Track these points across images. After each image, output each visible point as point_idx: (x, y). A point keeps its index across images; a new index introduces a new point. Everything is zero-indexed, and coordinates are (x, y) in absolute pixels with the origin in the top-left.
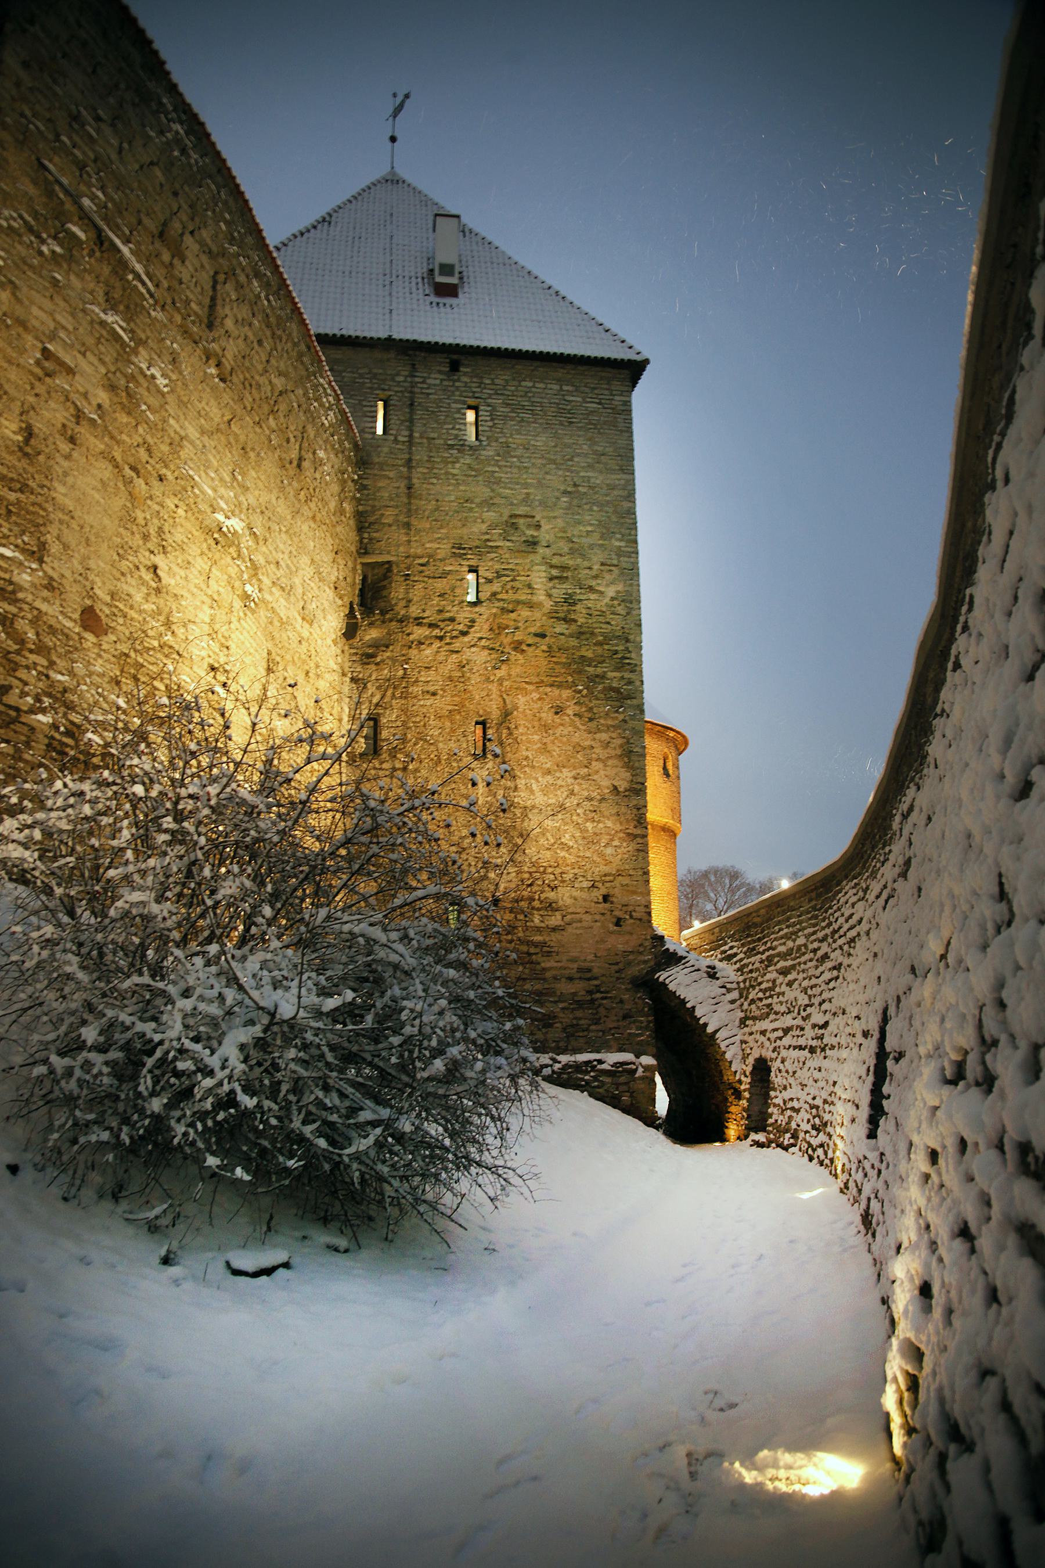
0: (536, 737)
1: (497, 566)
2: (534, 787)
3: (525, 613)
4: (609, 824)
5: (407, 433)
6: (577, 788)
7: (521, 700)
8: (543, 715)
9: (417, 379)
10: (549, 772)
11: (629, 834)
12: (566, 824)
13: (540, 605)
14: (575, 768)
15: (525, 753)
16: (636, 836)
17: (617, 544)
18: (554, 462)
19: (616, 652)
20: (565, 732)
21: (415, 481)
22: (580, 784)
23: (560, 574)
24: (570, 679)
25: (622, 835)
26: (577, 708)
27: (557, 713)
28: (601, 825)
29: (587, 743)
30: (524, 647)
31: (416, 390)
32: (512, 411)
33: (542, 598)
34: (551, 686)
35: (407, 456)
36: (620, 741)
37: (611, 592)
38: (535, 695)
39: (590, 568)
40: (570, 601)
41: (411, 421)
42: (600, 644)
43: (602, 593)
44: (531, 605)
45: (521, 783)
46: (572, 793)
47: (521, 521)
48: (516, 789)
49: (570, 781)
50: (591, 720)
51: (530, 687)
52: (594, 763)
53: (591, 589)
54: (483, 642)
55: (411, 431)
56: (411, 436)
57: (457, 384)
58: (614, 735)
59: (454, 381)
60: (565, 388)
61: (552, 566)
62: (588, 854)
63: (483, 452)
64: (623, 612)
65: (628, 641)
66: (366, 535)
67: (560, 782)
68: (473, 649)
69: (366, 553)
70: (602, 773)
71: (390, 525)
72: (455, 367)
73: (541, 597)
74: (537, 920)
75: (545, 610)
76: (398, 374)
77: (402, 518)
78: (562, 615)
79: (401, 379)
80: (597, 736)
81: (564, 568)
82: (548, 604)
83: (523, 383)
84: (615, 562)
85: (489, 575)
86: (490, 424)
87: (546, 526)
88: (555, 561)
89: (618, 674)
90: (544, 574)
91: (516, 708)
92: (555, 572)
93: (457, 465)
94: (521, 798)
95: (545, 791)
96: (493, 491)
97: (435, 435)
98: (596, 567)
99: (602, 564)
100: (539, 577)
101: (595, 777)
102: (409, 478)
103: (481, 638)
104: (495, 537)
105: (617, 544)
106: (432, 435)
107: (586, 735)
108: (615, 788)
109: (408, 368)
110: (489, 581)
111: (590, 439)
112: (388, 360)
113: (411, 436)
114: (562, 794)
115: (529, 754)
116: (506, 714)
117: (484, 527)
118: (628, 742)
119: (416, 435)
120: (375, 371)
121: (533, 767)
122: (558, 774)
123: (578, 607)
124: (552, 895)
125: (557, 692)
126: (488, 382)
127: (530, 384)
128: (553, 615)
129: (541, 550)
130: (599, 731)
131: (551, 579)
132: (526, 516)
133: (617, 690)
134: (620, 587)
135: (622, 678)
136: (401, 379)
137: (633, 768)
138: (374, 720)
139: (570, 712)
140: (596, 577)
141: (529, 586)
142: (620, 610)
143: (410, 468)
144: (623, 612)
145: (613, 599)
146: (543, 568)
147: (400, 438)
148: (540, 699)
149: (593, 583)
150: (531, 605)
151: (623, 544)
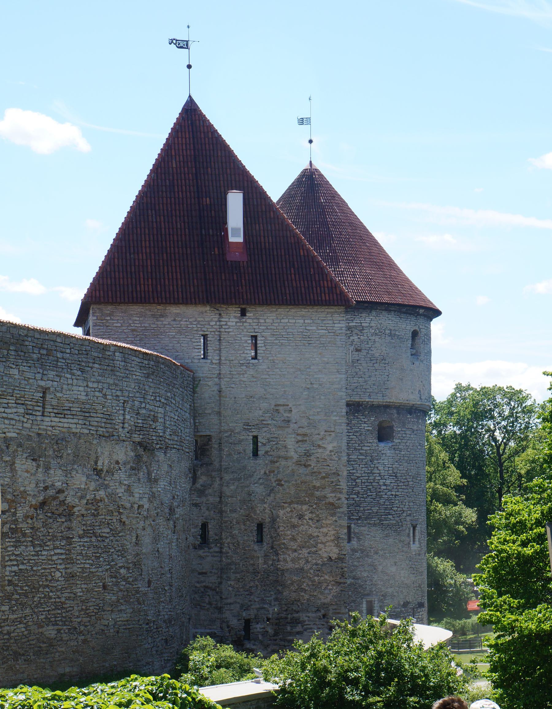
0: (289, 532)
1: (268, 436)
2: (288, 559)
3: (283, 463)
4: (327, 577)
5: (218, 358)
6: (310, 559)
7: (281, 513)
8: (293, 520)
9: (222, 323)
10: (295, 551)
11: (337, 582)
12: (304, 578)
13: (291, 458)
14: (309, 548)
15: (283, 541)
16: (340, 583)
17: (334, 418)
18: (300, 370)
19: (332, 482)
20: (304, 529)
21: (223, 386)
22: (311, 557)
23: (302, 439)
24: (307, 499)
25: (333, 583)
26: (310, 515)
27: (300, 518)
28: (322, 578)
29: (316, 534)
30: (283, 483)
31: (222, 330)
32: (276, 339)
33: (292, 453)
34: (298, 504)
35: (218, 372)
36: (333, 532)
37: (330, 447)
38: (288, 509)
39: (319, 434)
40: (308, 454)
41: (220, 350)
42: (323, 478)
43: (325, 448)
44: (286, 458)
45: (281, 557)
46: (307, 562)
47: (281, 408)
48: (279, 560)
49: (306, 555)
50: (318, 521)
51: (286, 505)
52: (319, 545)
53: (319, 446)
54: (261, 481)
55: (220, 356)
56: (220, 359)
57: (245, 324)
58: (330, 529)
59: (243, 322)
60: (306, 321)
61: (298, 435)
62: (315, 594)
63: (260, 367)
64: (337, 459)
65: (339, 475)
66: (197, 421)
67: (301, 556)
68: (256, 485)
69: (198, 431)
70: (323, 550)
71: (210, 414)
72: (243, 313)
73: (292, 453)
74: (289, 628)
75: (294, 461)
76: (212, 321)
77: (216, 409)
78: (303, 463)
79: (213, 323)
80: (321, 530)
81: (305, 435)
82: (296, 457)
83: (282, 321)
84: (332, 429)
85: (264, 441)
86: (264, 348)
87: (294, 411)
88: (300, 431)
89: (333, 495)
90: (293, 440)
91: (278, 517)
92: (300, 438)
93: (246, 376)
94: (281, 565)
95: (293, 560)
96: (265, 390)
97: (234, 358)
98: (322, 433)
99: (325, 431)
100: (291, 442)
101: (320, 552)
102: (219, 385)
103: (260, 479)
104: (267, 419)
105: (334, 418)
106: (231, 358)
107: (315, 530)
108: (330, 558)
109: (217, 316)
110: (264, 445)
111: (320, 354)
112: (206, 312)
113: (220, 359)
114: (302, 562)
115: (285, 541)
116: (274, 520)
117: (261, 412)
118: (338, 533)
119: (223, 358)
120: (199, 319)
121: (287, 548)
122: (300, 552)
123: (312, 458)
124: (295, 615)
125: (300, 507)
126: (262, 321)
127: (287, 321)
128: (298, 463)
129: (292, 425)
130: (322, 527)
131: (297, 442)
132: (284, 405)
133: (332, 504)
134: (335, 444)
135: (335, 497)
136: (213, 323)
137: (340, 547)
138: (204, 526)
139: (307, 518)
140: (322, 439)
141: (285, 447)
142: (334, 457)
143: (220, 378)
144: (337, 459)
145: (331, 451)
146: (293, 436)
147: (214, 361)
148: (291, 511)
149: (320, 443)
150: (286, 458)
151: (337, 418)
